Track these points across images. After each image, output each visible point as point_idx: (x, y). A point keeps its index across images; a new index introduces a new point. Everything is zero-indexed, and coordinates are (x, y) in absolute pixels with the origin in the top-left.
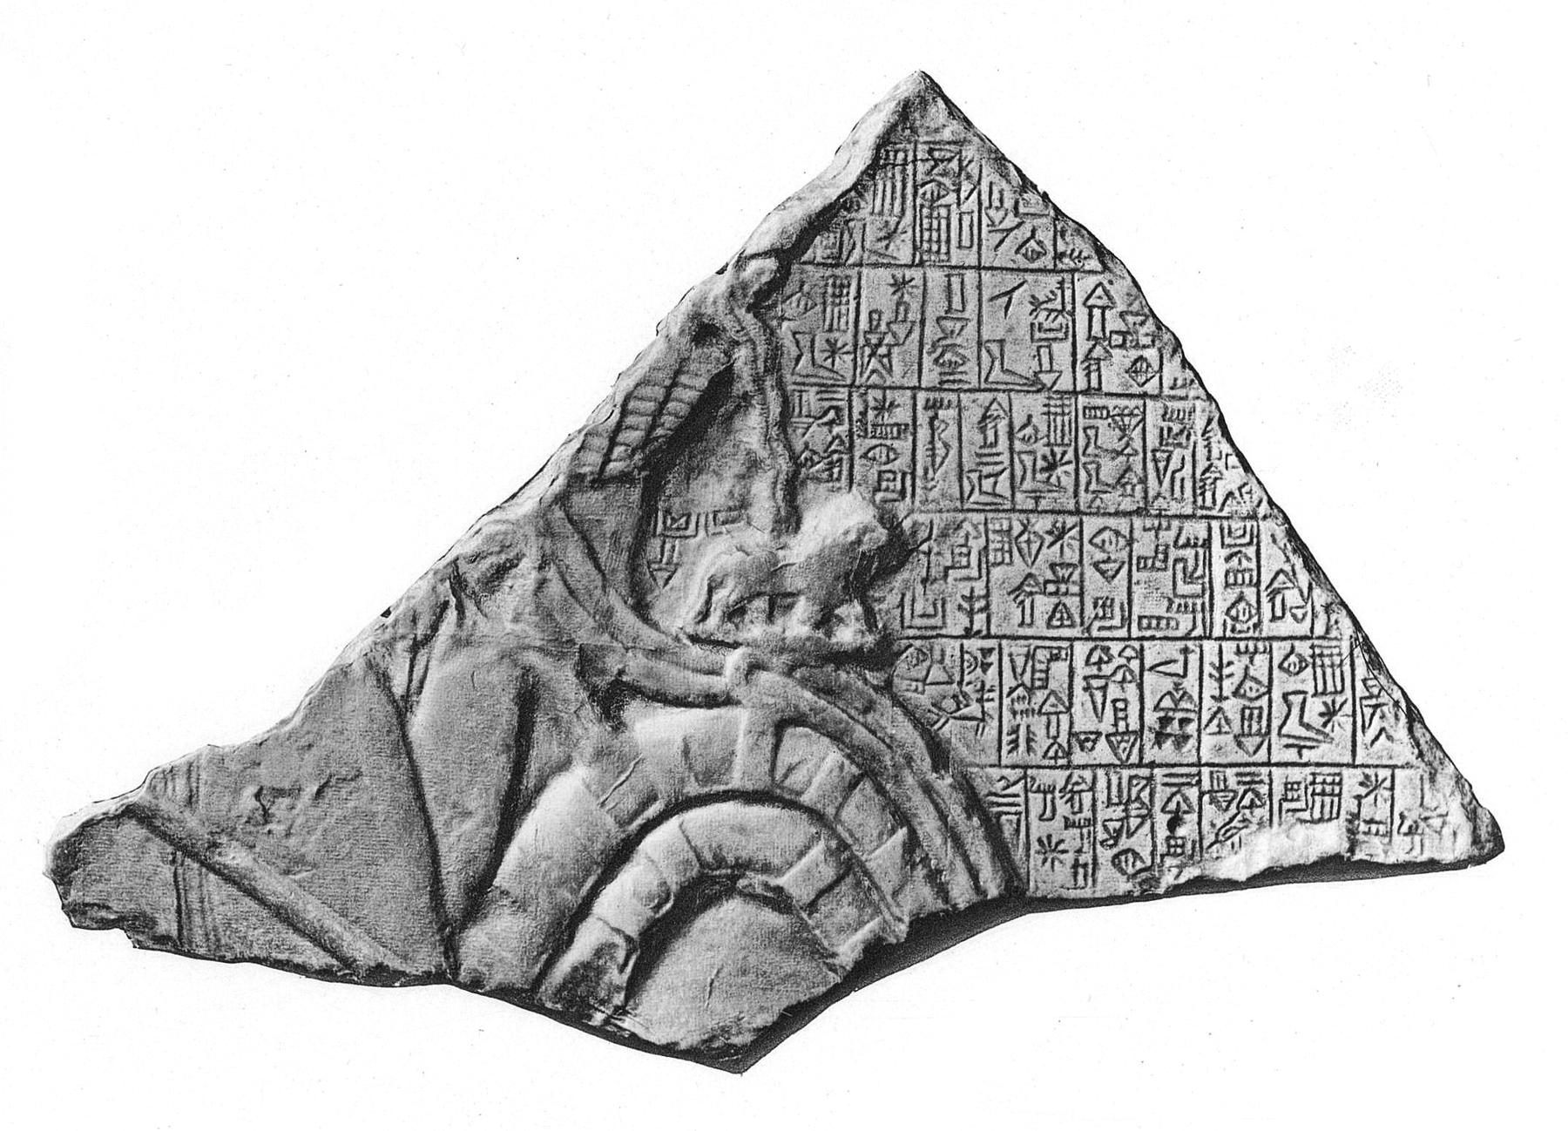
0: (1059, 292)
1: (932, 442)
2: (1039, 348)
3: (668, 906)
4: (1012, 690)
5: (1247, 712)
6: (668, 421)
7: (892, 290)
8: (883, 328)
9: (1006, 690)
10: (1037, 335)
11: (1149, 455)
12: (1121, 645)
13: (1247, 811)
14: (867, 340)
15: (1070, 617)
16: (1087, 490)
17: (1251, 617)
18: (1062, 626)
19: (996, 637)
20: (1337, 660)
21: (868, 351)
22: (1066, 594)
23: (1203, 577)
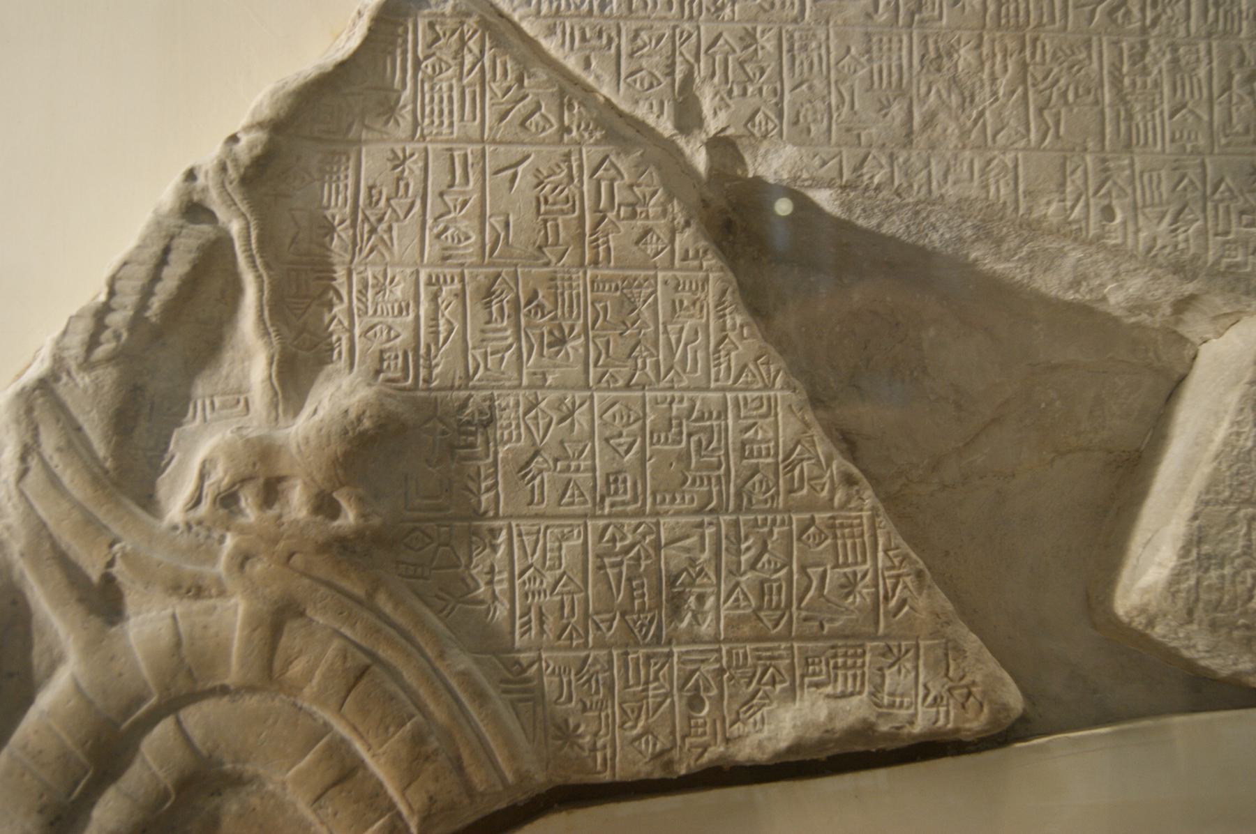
0: (564, 166)
1: (436, 319)
2: (545, 221)
3: (168, 805)
4: (522, 573)
5: (766, 586)
6: (156, 303)
7: (389, 165)
8: (383, 203)
9: (517, 572)
10: (543, 209)
11: (661, 327)
12: (634, 522)
13: (768, 688)
14: (366, 218)
15: (582, 495)
16: (596, 365)
17: (768, 490)
18: (572, 503)
19: (504, 517)
20: (856, 531)
21: (367, 227)
22: (578, 470)
23: (718, 449)
